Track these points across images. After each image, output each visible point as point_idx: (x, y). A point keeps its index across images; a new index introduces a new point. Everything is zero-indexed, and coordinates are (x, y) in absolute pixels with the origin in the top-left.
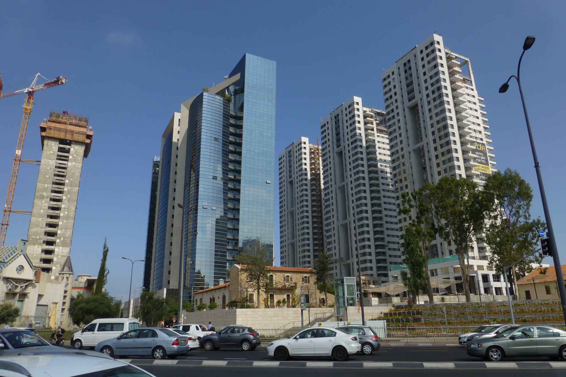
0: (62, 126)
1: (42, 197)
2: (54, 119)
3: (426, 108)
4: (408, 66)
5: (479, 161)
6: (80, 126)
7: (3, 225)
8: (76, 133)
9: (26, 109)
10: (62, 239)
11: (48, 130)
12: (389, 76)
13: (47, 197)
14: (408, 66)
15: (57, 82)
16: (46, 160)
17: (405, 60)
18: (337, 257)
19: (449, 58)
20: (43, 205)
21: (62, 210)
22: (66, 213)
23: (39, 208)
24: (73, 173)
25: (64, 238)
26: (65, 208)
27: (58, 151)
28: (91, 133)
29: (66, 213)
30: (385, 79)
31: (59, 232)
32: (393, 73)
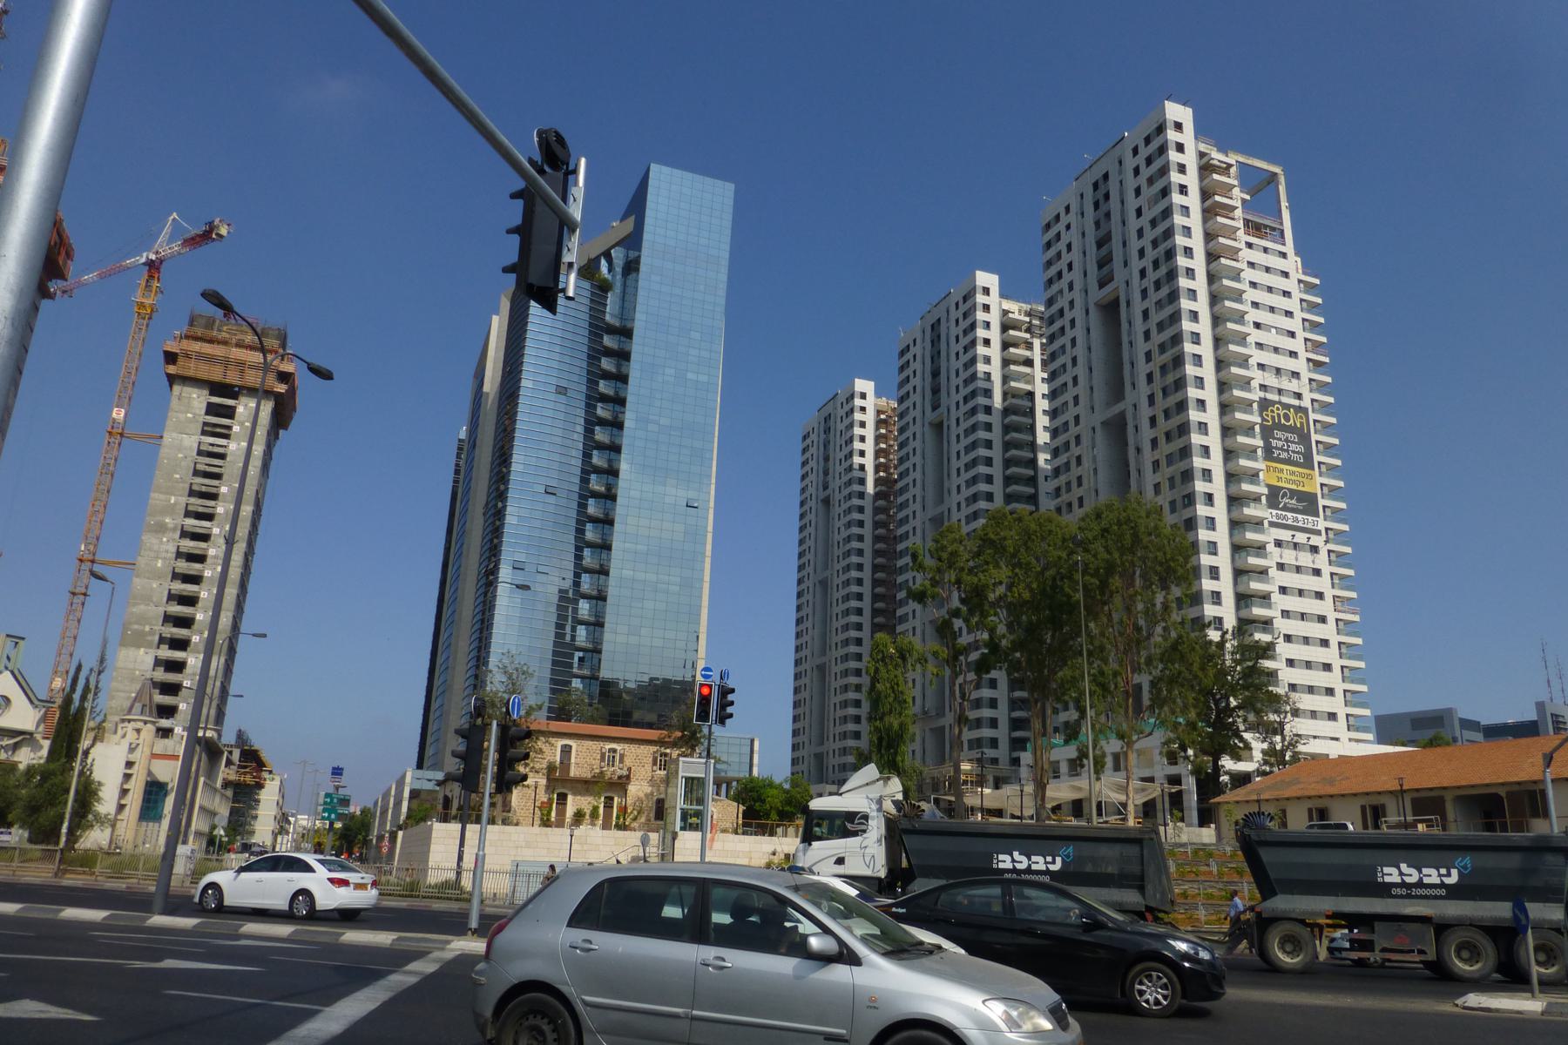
0: (218, 351)
1: (161, 529)
2: (199, 332)
3: (1138, 307)
4: (1102, 191)
5: (1284, 455)
7: (74, 594)
8: (251, 367)
9: (142, 305)
11: (181, 361)
12: (1058, 218)
13: (174, 530)
14: (1102, 191)
15: (207, 235)
16: (174, 435)
17: (1097, 174)
18: (917, 709)
19: (1206, 168)
20: (164, 547)
27: (207, 413)
30: (1048, 226)
32: (1068, 209)
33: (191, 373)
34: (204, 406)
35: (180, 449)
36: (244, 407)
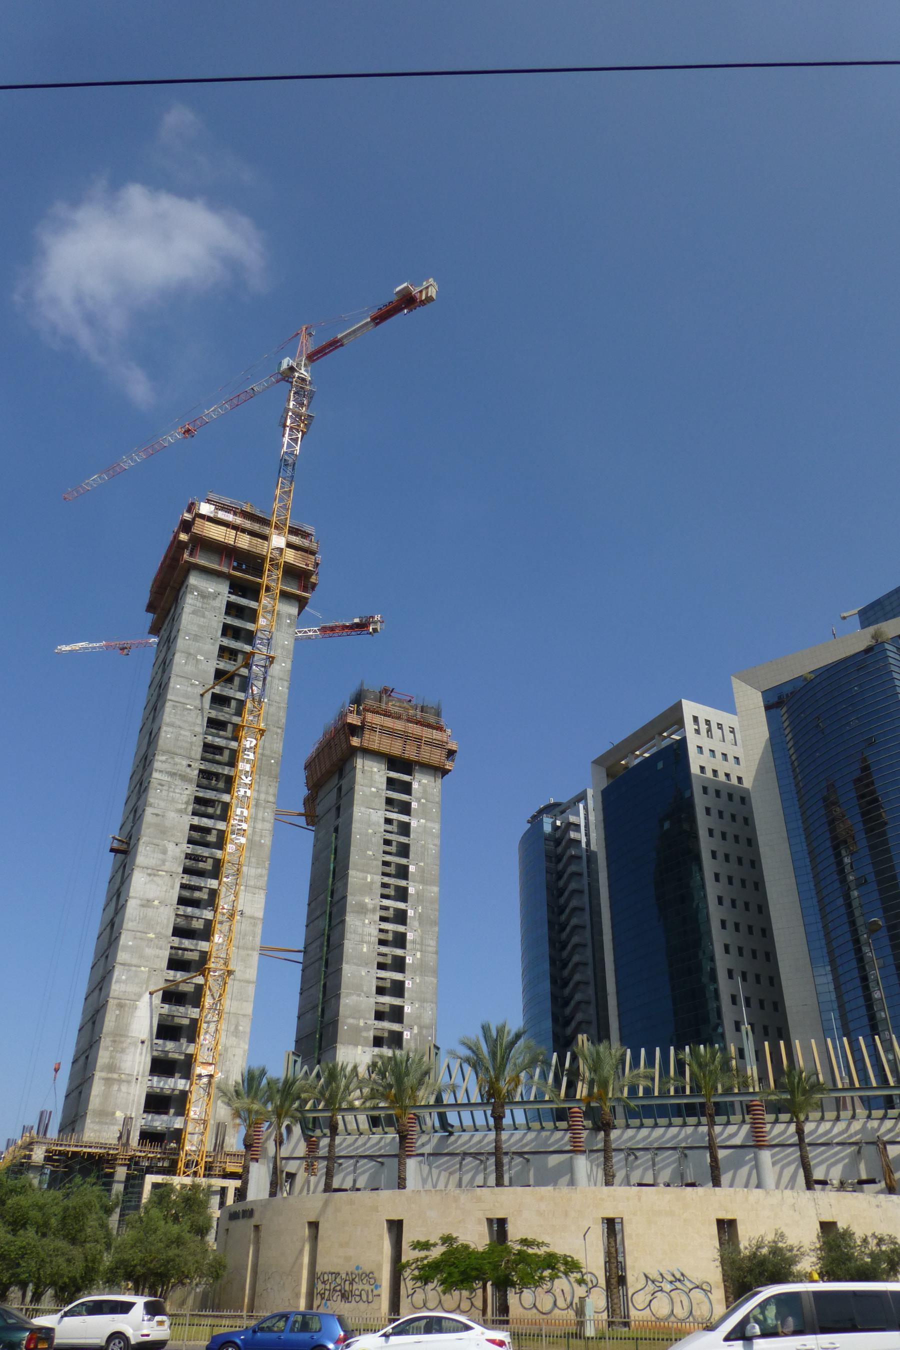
0: (399, 725)
1: (362, 910)
6: (429, 726)
8: (427, 743)
10: (416, 1030)
13: (374, 910)
16: (363, 809)
21: (408, 946)
22: (418, 955)
23: (358, 938)
24: (423, 846)
25: (421, 1028)
26: (414, 942)
28: (453, 746)
29: (418, 955)
31: (407, 1009)
33: (375, 746)
34: (384, 780)
35: (369, 824)
36: (421, 782)
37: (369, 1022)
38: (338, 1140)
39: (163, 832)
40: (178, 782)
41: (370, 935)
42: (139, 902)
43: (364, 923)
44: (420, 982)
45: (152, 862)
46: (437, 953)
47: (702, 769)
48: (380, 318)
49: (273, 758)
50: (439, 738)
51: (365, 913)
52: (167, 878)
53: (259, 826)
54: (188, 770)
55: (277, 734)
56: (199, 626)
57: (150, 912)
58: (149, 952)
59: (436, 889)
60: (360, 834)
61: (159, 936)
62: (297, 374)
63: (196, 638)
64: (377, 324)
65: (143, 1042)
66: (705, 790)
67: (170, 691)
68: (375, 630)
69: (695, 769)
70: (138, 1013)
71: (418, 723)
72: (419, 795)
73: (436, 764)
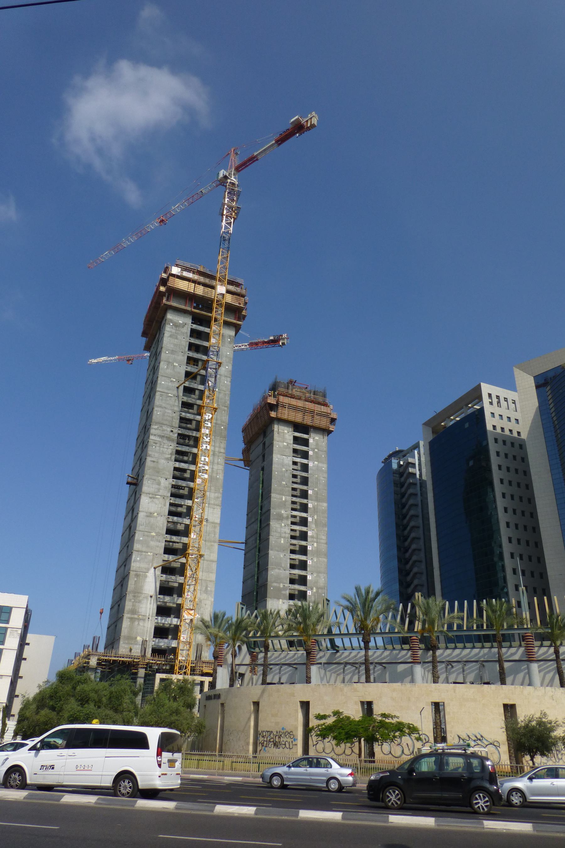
0: (300, 403)
1: (280, 518)
6: (319, 403)
10: (315, 590)
13: (287, 518)
16: (279, 456)
21: (309, 539)
22: (315, 545)
23: (278, 535)
24: (317, 478)
25: (318, 588)
26: (312, 537)
28: (334, 416)
29: (315, 545)
31: (309, 578)
33: (285, 417)
34: (292, 438)
35: (283, 465)
36: (314, 439)
37: (286, 585)
38: (269, 654)
39: (157, 471)
40: (166, 441)
41: (285, 533)
42: (145, 514)
43: (281, 526)
44: (317, 561)
45: (152, 490)
46: (326, 544)
47: (494, 427)
48: (281, 141)
49: (223, 425)
50: (325, 411)
51: (282, 520)
52: (161, 500)
53: (216, 467)
54: (171, 434)
55: (224, 410)
56: (175, 345)
57: (152, 520)
58: (152, 543)
59: (325, 505)
60: (277, 472)
61: (158, 534)
62: (229, 181)
63: (173, 352)
64: (280, 144)
65: (151, 597)
66: (496, 440)
67: (158, 386)
68: (283, 344)
69: (489, 427)
70: (148, 580)
71: (312, 402)
72: (313, 447)
73: (324, 427)
